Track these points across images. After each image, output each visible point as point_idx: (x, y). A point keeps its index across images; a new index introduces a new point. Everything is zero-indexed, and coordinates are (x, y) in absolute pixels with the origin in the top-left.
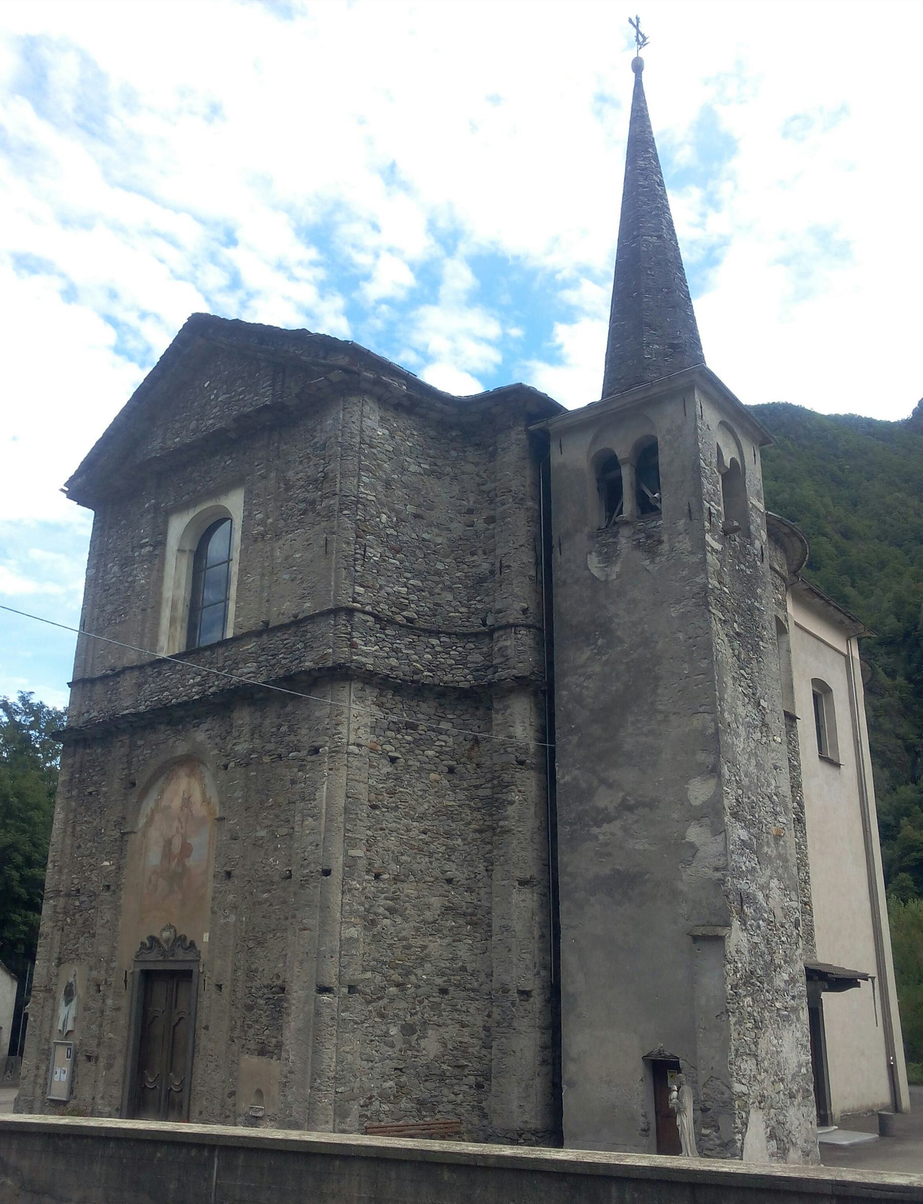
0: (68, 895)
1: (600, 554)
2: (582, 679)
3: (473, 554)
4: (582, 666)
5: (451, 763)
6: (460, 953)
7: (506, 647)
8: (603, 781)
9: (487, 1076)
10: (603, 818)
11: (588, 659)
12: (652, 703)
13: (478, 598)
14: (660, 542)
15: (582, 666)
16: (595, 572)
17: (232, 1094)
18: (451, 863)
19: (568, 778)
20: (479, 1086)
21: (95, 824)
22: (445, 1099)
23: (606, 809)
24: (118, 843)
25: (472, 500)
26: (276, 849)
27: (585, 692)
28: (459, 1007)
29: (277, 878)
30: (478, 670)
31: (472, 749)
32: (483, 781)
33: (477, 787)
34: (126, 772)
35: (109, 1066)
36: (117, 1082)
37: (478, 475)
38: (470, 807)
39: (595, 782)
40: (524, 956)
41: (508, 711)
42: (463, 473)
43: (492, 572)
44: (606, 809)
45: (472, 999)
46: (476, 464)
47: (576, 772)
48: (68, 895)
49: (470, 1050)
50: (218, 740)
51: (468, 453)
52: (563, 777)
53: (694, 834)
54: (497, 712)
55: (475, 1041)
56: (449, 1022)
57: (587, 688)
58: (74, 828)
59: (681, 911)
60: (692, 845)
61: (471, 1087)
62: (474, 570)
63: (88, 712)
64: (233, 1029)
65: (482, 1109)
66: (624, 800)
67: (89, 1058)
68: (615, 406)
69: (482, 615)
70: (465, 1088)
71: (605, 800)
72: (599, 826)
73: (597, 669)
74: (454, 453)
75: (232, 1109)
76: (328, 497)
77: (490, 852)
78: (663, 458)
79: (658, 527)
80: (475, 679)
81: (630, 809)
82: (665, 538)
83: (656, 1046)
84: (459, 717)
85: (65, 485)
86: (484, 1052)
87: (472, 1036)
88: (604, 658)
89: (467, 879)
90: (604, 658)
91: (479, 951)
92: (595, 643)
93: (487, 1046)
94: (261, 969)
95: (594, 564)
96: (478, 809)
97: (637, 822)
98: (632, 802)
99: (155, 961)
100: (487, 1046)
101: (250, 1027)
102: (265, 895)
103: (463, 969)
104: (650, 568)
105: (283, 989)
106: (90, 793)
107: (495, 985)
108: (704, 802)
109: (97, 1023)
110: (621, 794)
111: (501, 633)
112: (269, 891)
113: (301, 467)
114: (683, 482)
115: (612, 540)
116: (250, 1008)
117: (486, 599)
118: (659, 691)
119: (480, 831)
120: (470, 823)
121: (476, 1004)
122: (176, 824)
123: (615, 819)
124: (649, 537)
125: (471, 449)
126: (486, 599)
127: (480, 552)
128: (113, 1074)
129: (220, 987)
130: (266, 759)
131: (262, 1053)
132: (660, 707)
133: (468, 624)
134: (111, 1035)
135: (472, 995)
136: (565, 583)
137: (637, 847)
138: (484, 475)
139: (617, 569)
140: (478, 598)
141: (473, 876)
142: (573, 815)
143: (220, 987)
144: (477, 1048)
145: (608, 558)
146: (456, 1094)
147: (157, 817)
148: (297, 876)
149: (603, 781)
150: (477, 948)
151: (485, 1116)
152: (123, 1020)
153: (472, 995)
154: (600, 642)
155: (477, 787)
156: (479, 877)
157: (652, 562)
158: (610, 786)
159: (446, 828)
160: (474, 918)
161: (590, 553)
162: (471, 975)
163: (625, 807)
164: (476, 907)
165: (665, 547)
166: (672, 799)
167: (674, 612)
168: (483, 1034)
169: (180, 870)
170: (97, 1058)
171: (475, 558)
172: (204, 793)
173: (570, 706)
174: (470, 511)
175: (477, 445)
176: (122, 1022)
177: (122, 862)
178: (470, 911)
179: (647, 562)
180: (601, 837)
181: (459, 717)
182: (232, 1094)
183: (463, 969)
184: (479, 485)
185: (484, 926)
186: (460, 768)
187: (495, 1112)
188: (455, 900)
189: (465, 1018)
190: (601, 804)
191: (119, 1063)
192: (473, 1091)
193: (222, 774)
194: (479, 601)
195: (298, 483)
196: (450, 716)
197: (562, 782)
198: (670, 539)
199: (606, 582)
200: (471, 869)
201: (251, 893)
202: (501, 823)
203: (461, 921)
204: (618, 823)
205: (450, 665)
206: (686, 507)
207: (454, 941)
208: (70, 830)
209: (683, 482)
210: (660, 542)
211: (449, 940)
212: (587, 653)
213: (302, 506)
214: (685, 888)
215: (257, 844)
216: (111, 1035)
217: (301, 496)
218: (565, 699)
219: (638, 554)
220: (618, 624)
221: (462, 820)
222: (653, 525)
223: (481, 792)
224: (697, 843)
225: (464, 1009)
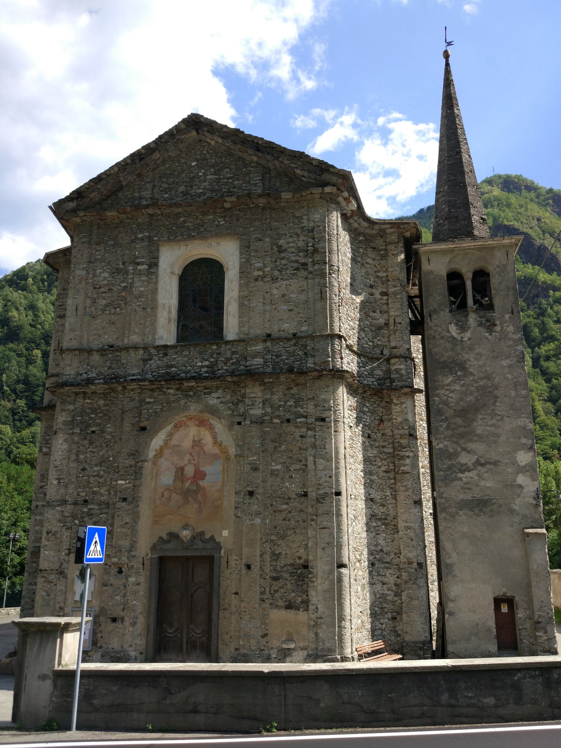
0: (75, 503)
1: (457, 325)
2: (448, 392)
3: (374, 312)
4: (448, 385)
5: (370, 432)
6: (380, 542)
7: (401, 369)
8: (464, 449)
9: (399, 612)
10: (465, 469)
11: (451, 382)
12: (493, 410)
13: (378, 338)
14: (495, 325)
15: (448, 385)
16: (454, 334)
17: (264, 636)
18: (372, 489)
19: (441, 446)
20: (394, 618)
21: (101, 453)
22: (377, 628)
23: (467, 464)
24: (133, 468)
25: (372, 279)
26: (291, 477)
27: (450, 400)
28: (381, 573)
29: (294, 496)
30: (380, 380)
31: (379, 424)
32: (387, 443)
33: (384, 447)
34: (138, 419)
35: (134, 624)
36: (140, 634)
37: (375, 266)
38: (380, 458)
39: (459, 449)
40: (420, 543)
41: (404, 406)
42: (367, 263)
43: (387, 324)
44: (467, 464)
45: (388, 568)
46: (374, 260)
47: (446, 443)
48: (75, 503)
49: (388, 598)
50: (230, 405)
51: (368, 252)
52: (438, 445)
53: (521, 479)
54: (396, 405)
55: (390, 592)
56: (377, 582)
57: (452, 398)
58: (77, 455)
59: (515, 520)
60: (520, 486)
61: (389, 620)
62: (375, 321)
63: (86, 373)
64: (262, 593)
65: (396, 631)
66: (478, 460)
67: (114, 620)
68: (464, 245)
69: (381, 348)
70: (386, 620)
71: (465, 459)
72: (462, 473)
73: (458, 388)
74: (361, 250)
75: (266, 645)
76: (319, 264)
77: (395, 484)
78: (494, 281)
79: (493, 316)
80: (379, 384)
81: (482, 465)
82: (498, 323)
83: (501, 591)
84: (371, 405)
85: (54, 204)
86: (396, 598)
87: (388, 590)
88: (462, 382)
89: (381, 499)
90: (462, 382)
91: (390, 540)
92: (456, 373)
93: (398, 594)
94: (284, 553)
95: (453, 330)
96: (385, 460)
97: (487, 472)
98: (483, 461)
99: (171, 550)
100: (398, 594)
101: (276, 591)
102: (284, 507)
103: (382, 551)
104: (490, 337)
105: (306, 567)
106: (93, 432)
107: (403, 559)
108: (526, 464)
109: (121, 594)
110: (476, 457)
111: (397, 360)
112: (287, 504)
113: (291, 240)
114: (508, 295)
115: (464, 319)
116: (275, 579)
117: (382, 339)
118: (497, 404)
119: (386, 472)
120: (380, 467)
121: (390, 571)
122: (188, 457)
123: (472, 470)
124: (488, 321)
125: (370, 250)
126: (382, 339)
127: (378, 311)
128: (135, 630)
129: (249, 567)
130: (276, 421)
131: (289, 606)
132: (498, 412)
133: (373, 352)
134: (135, 602)
135: (387, 566)
136: (434, 337)
137: (487, 485)
138: (378, 267)
139: (468, 334)
140: (378, 338)
141: (384, 497)
142: (445, 466)
143: (249, 567)
144: (392, 596)
145: (463, 328)
146: (382, 624)
147: (166, 451)
148: (312, 495)
149: (464, 449)
150: (388, 538)
151: (398, 635)
152: (142, 591)
153: (387, 566)
154: (459, 373)
155: (384, 447)
156: (387, 498)
157: (491, 334)
158: (469, 452)
159: (370, 469)
160: (386, 521)
161: (451, 324)
162: (386, 554)
163: (478, 463)
164: (387, 515)
165: (498, 328)
166: (507, 461)
167: (505, 363)
168: (394, 588)
169: (194, 488)
170: (123, 619)
171: (375, 314)
172: (215, 438)
173: (440, 406)
174: (371, 287)
175: (374, 248)
176: (142, 593)
177: (137, 482)
178: (383, 517)
179: (487, 334)
180: (464, 479)
181: (371, 405)
182: (264, 636)
183: (382, 551)
184: (375, 272)
185: (392, 526)
186: (373, 436)
187: (406, 633)
188: (376, 511)
189: (386, 580)
190: (463, 461)
191: (141, 620)
192: (390, 622)
193: (237, 427)
194: (379, 340)
195: (290, 250)
196: (367, 405)
197: (437, 447)
198: (501, 324)
199: (462, 341)
200: (382, 493)
201: (272, 505)
202: (402, 468)
203: (379, 523)
204: (475, 472)
205: (366, 375)
206: (510, 309)
207: (376, 534)
208: (73, 457)
209: (508, 295)
210: (495, 325)
211: (374, 534)
212: (451, 378)
213: (296, 265)
214: (517, 508)
215: (274, 473)
216: (135, 602)
217: (294, 259)
218: (437, 402)
219: (481, 329)
220: (470, 365)
221: (376, 465)
222: (490, 314)
223: (385, 450)
224: (523, 485)
225: (383, 574)
